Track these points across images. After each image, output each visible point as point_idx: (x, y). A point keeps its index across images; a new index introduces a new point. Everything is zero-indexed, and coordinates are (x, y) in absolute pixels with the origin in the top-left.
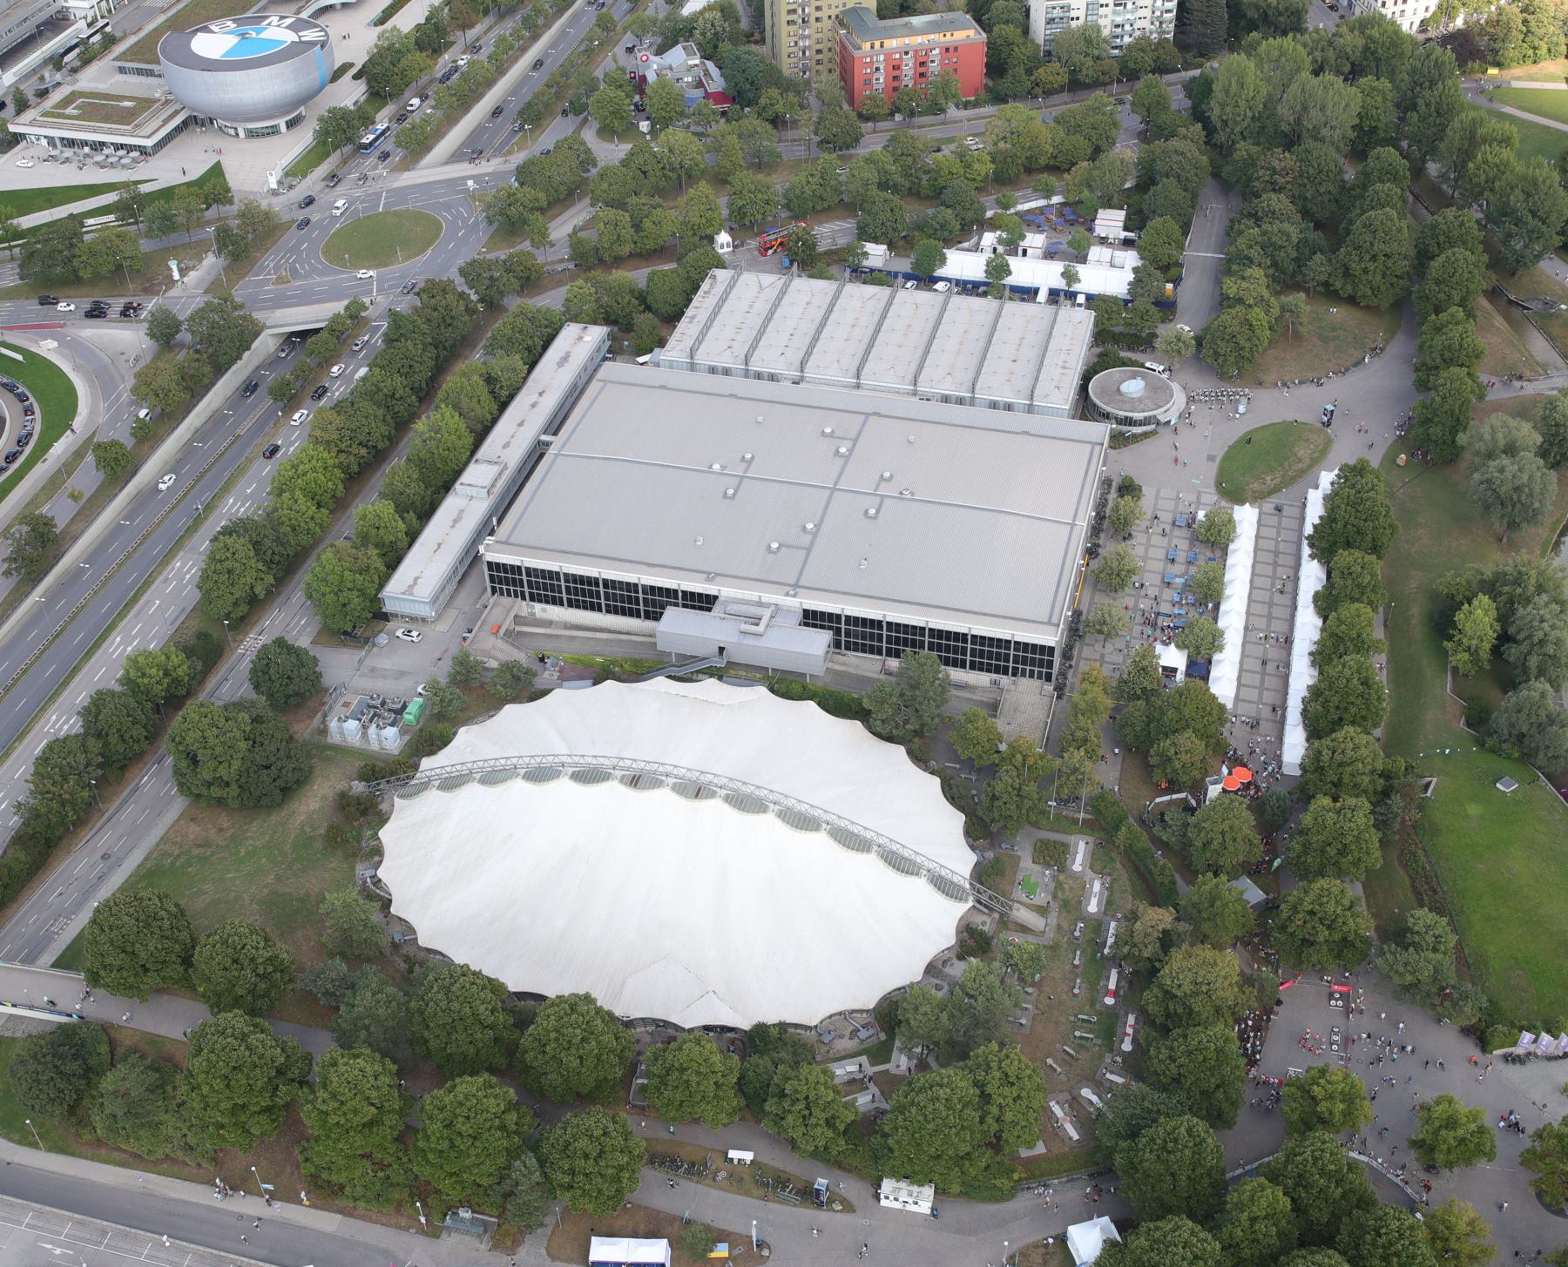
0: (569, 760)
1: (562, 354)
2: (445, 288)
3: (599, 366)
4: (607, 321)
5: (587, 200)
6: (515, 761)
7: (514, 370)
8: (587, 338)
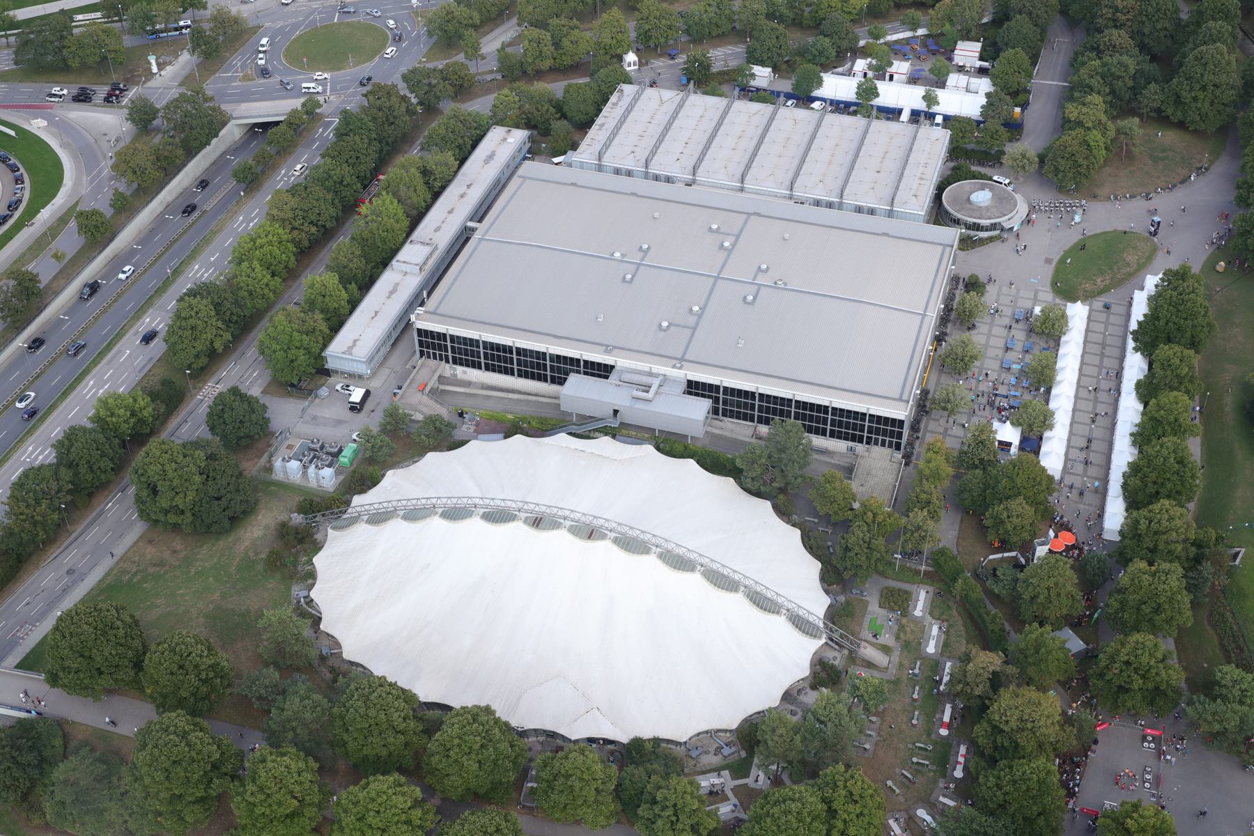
0: (481, 502)
1: (489, 153)
2: (390, 91)
3: (520, 164)
4: (528, 125)
5: (515, 20)
6: (434, 501)
7: (446, 165)
8: (510, 140)
